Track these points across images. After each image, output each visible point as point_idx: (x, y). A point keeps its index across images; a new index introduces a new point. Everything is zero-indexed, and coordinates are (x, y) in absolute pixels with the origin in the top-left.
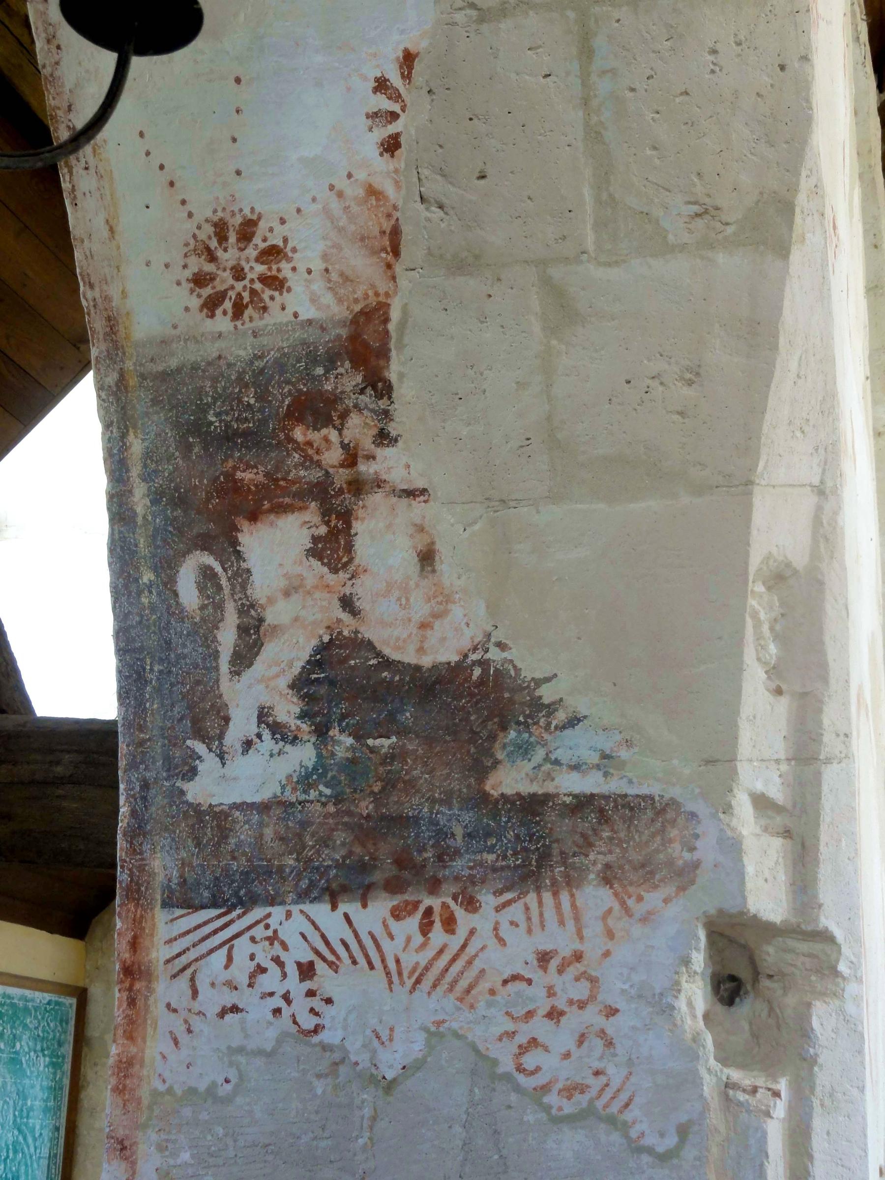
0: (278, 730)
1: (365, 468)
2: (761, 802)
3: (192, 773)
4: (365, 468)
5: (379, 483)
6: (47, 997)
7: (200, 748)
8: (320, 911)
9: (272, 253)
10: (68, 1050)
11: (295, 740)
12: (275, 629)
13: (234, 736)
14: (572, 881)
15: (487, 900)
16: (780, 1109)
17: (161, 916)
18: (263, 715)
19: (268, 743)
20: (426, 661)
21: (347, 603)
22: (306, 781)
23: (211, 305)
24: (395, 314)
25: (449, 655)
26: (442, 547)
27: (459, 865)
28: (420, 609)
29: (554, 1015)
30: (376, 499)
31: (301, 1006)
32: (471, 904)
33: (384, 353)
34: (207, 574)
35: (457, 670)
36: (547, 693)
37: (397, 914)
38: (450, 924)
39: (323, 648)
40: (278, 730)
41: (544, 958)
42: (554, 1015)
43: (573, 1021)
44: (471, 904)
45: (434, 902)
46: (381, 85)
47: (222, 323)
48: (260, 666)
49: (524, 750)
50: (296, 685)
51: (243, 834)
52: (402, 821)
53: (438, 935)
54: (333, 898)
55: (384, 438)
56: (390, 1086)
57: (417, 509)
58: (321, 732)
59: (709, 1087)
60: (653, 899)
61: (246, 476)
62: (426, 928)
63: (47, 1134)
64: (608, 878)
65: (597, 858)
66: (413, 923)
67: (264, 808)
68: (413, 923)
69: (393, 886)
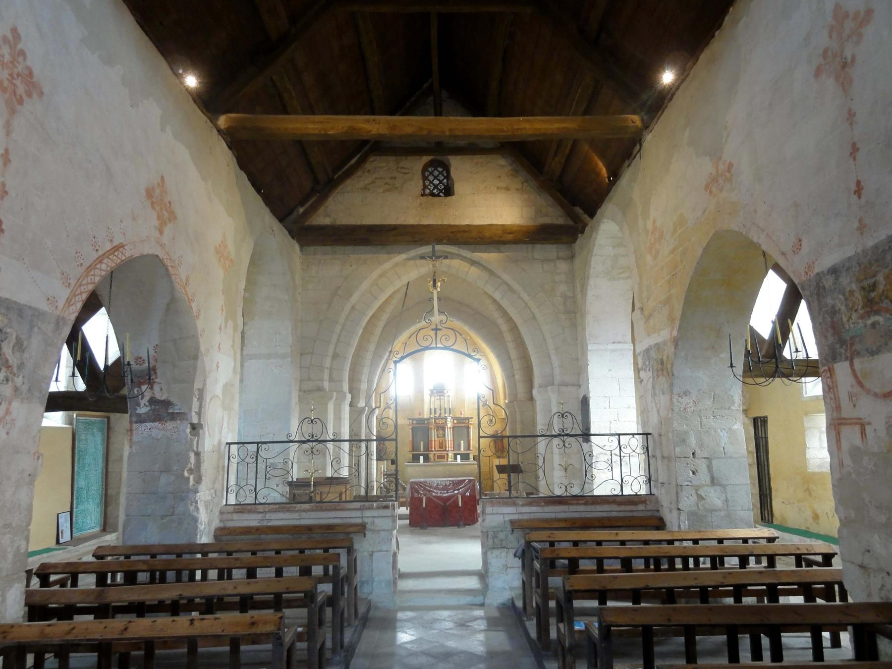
0: (146, 406)
1: (155, 381)
2: (196, 412)
3: (137, 410)
4: (155, 381)
5: (156, 382)
6: (100, 419)
7: (137, 407)
8: (151, 423)
9: (143, 360)
10: (106, 430)
11: (148, 407)
12: (146, 396)
13: (141, 407)
14: (177, 420)
15: (168, 422)
16: (196, 440)
17: (134, 424)
18: (145, 404)
19: (145, 407)
20: (162, 399)
21: (153, 393)
22: (149, 410)
23: (137, 364)
24: (157, 367)
25: (164, 399)
26: (163, 388)
27: (165, 419)
28: (161, 394)
29: (175, 432)
30: (156, 384)
31: (149, 432)
32: (167, 423)
33: (156, 370)
34: (138, 390)
35: (164, 400)
36: (174, 403)
37: (159, 423)
38: (164, 424)
39: (151, 398)
40: (146, 406)
41: (174, 427)
42: (175, 432)
43: (177, 433)
44: (167, 423)
45: (162, 422)
46: (154, 347)
47: (138, 366)
48: (144, 399)
49: (171, 408)
50: (148, 401)
51: (143, 416)
52: (159, 415)
53: (163, 425)
54: (153, 422)
55: (156, 378)
56: (158, 440)
57: (160, 385)
58: (151, 406)
59: (189, 438)
60: (184, 421)
61: (142, 381)
62: (162, 425)
63: (102, 449)
64: (180, 420)
65: (179, 418)
66: (161, 424)
67: (146, 413)
68: (161, 424)
69: (158, 421)
